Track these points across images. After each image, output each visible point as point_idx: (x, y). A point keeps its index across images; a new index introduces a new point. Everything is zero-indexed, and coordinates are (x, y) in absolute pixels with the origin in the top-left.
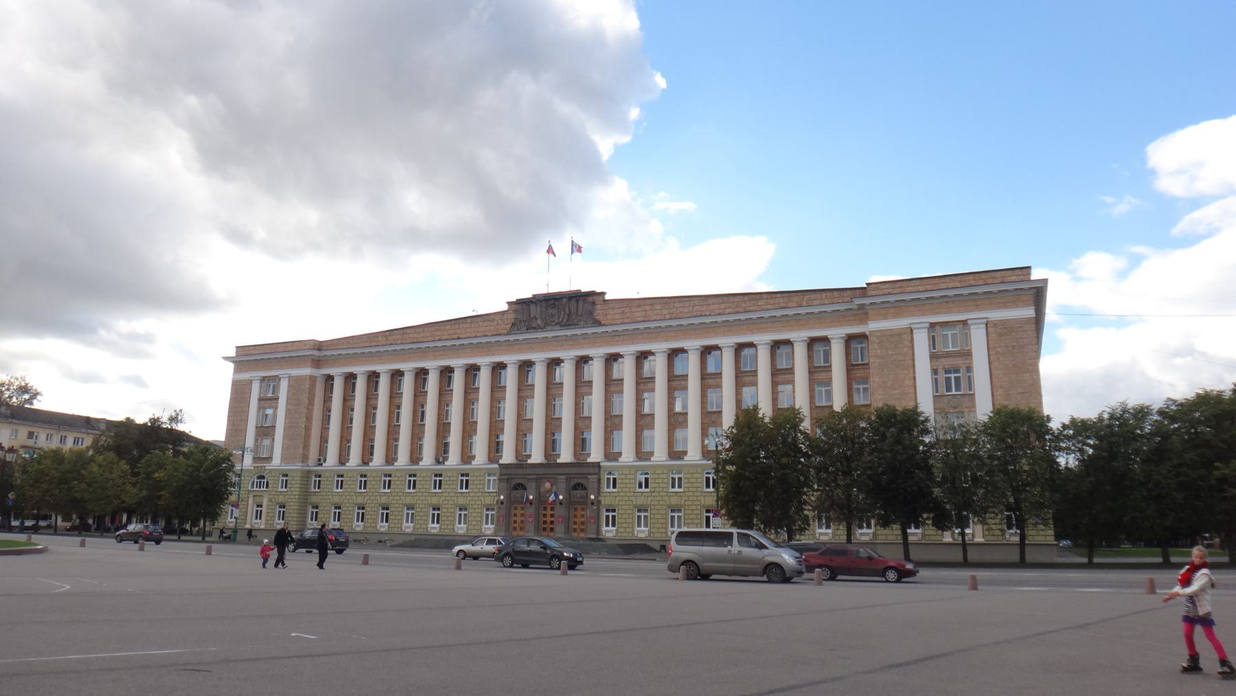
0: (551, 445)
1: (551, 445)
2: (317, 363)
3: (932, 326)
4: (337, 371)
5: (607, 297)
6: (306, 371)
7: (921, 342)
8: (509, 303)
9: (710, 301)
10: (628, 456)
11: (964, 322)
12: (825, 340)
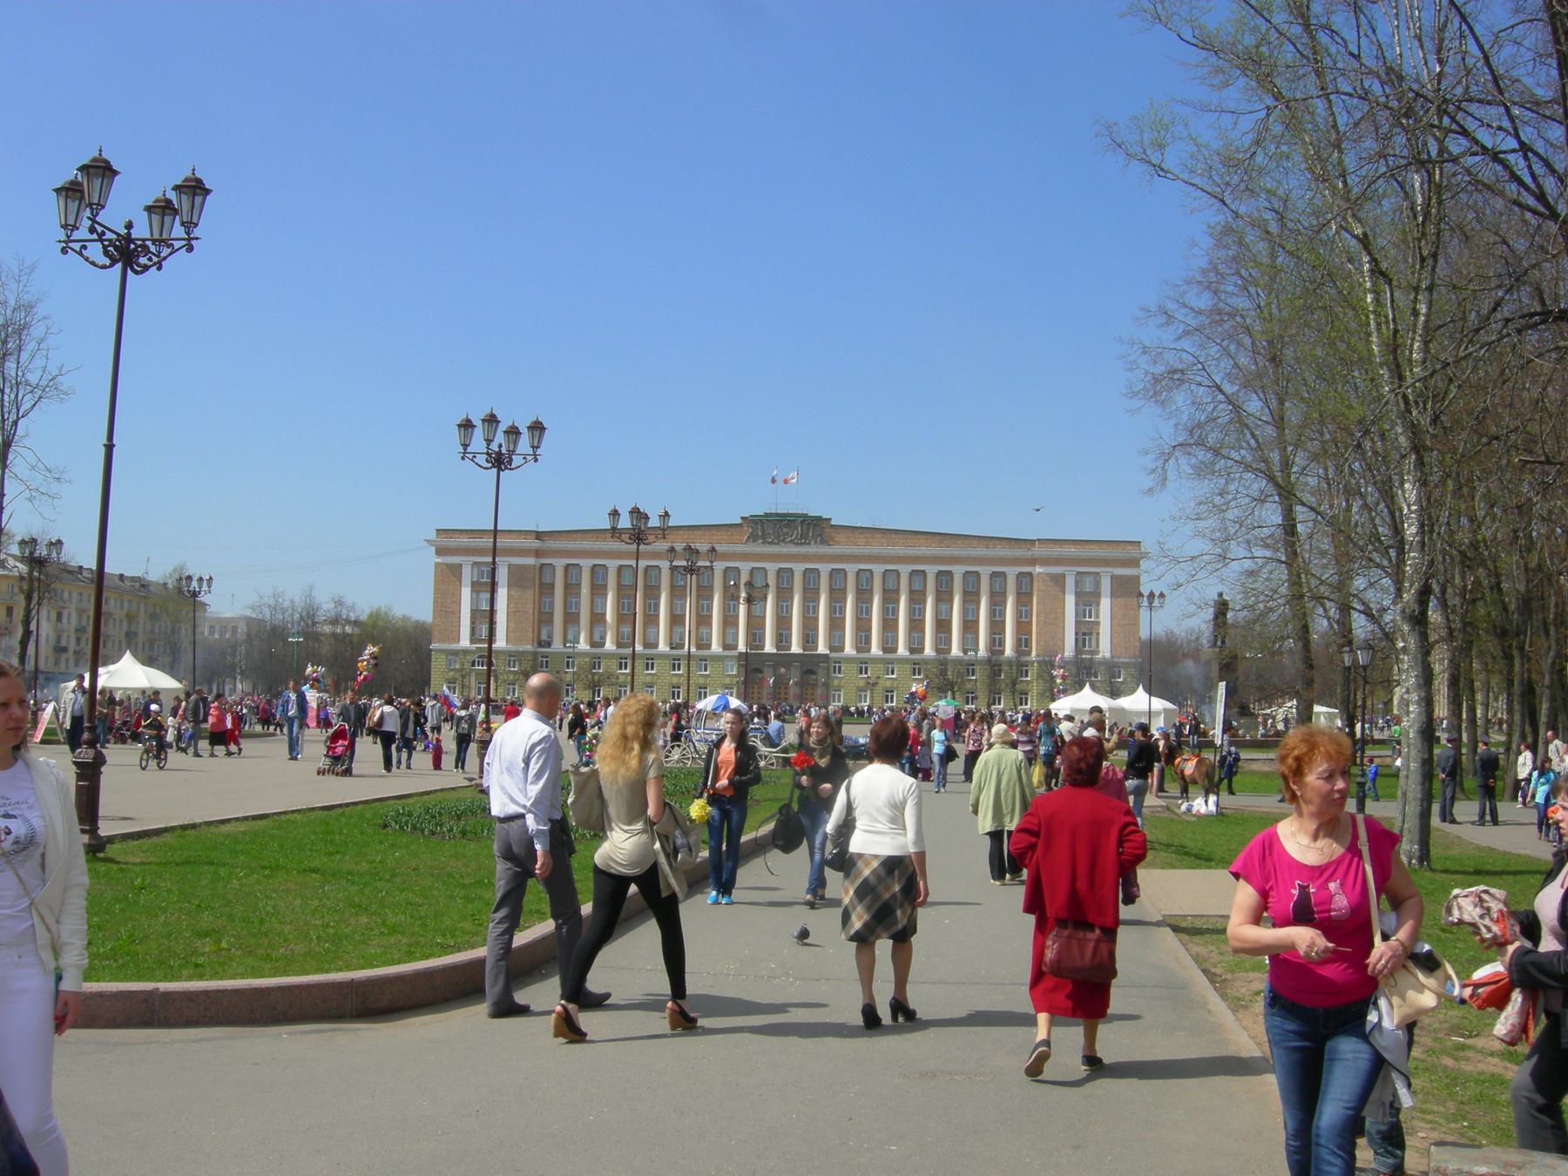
0: (782, 638)
1: (782, 638)
2: (538, 553)
3: (1078, 573)
4: (560, 563)
5: (832, 523)
6: (530, 561)
7: (1070, 582)
8: (742, 518)
9: (918, 537)
10: (849, 650)
11: (1098, 573)
12: (1003, 575)
